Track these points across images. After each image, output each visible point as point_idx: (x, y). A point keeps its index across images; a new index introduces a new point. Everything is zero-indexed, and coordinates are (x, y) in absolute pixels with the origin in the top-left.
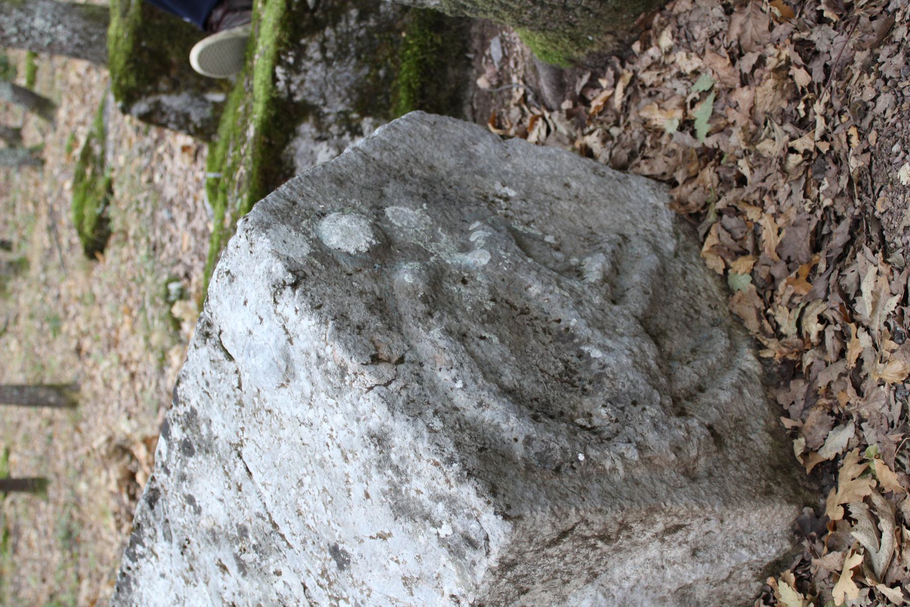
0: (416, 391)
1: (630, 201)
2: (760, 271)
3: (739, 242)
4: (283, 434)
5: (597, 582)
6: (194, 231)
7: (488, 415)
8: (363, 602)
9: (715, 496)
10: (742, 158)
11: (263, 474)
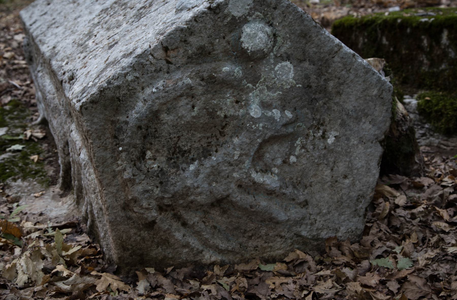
0: (150, 69)
7: (140, 104)
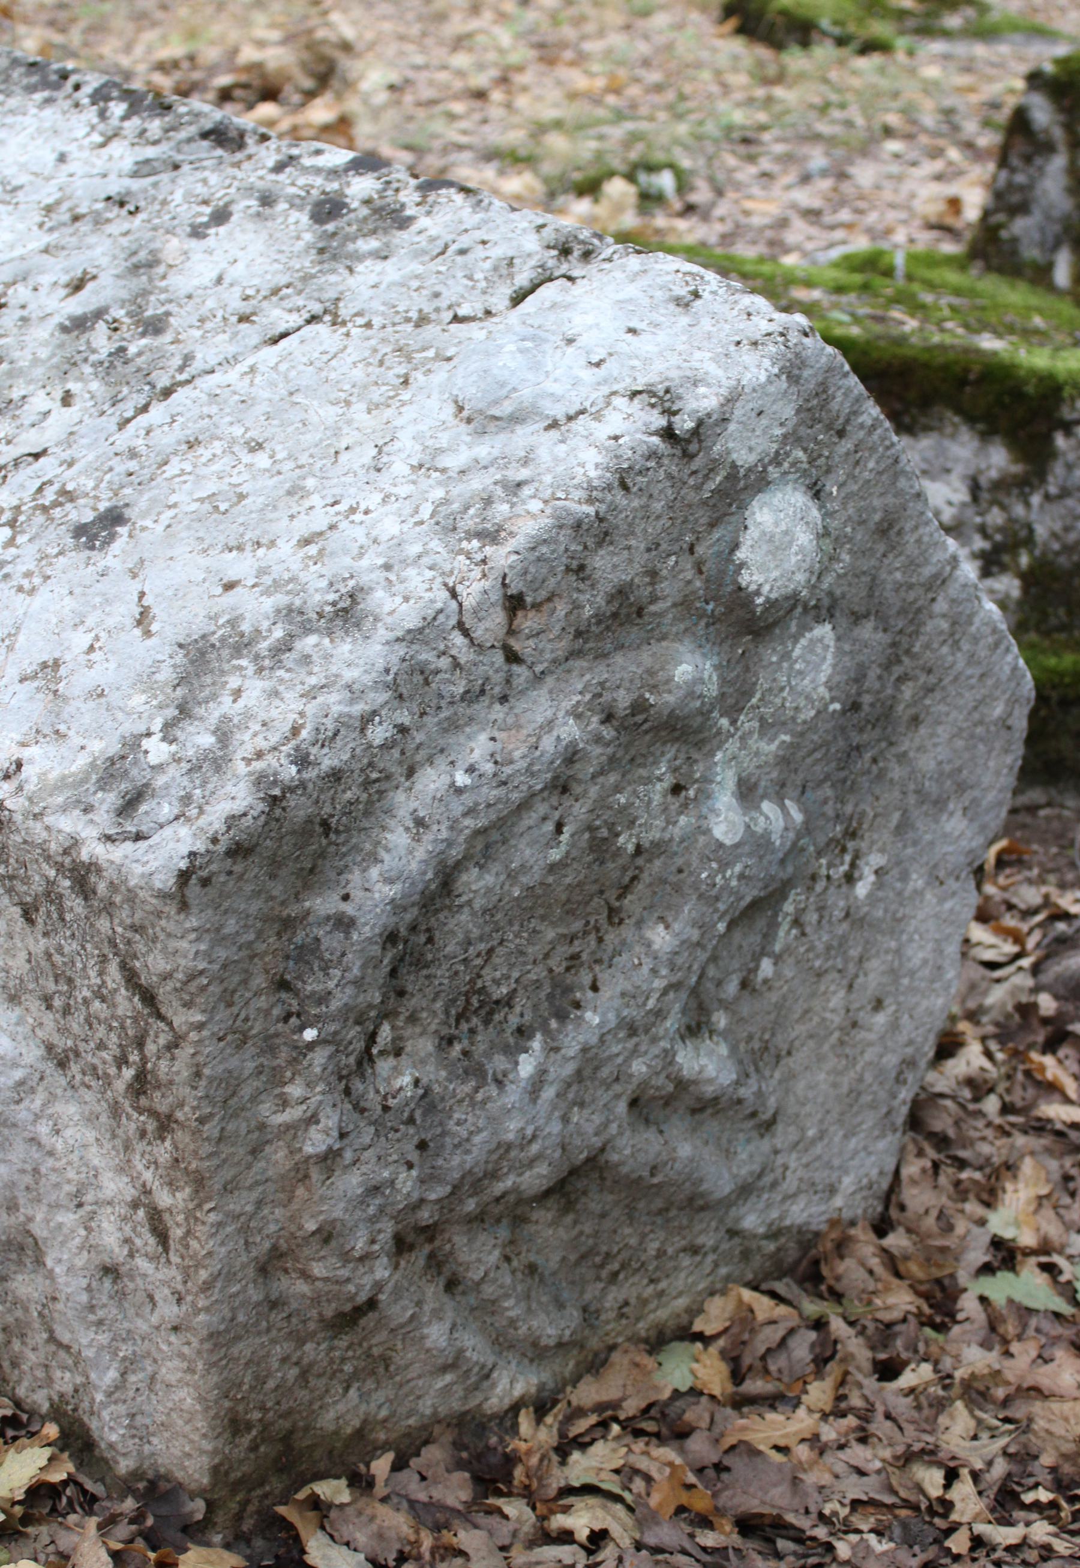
0: (448, 689)
1: (846, 1137)
2: (698, 1409)
3: (758, 1364)
4: (358, 409)
5: (49, 1067)
6: (783, 223)
7: (398, 838)
8: (7, 576)
9: (229, 1315)
10: (936, 1371)
11: (275, 368)
